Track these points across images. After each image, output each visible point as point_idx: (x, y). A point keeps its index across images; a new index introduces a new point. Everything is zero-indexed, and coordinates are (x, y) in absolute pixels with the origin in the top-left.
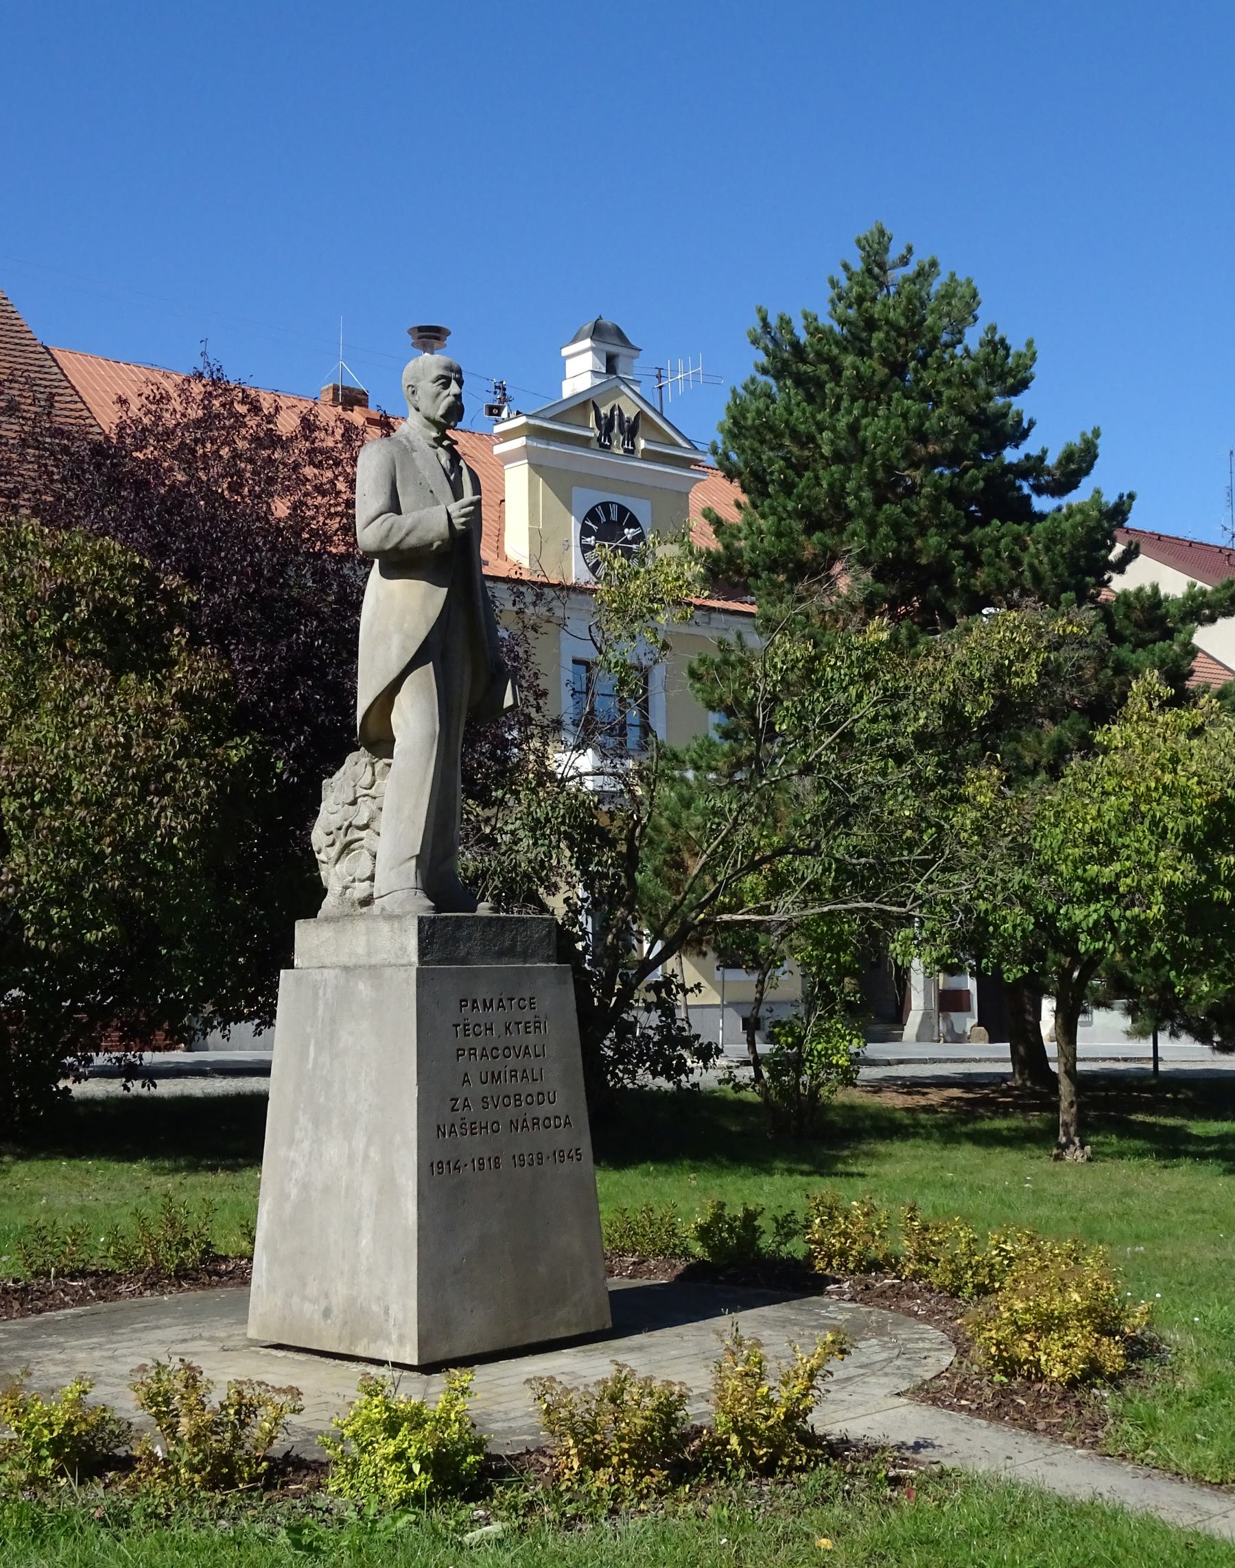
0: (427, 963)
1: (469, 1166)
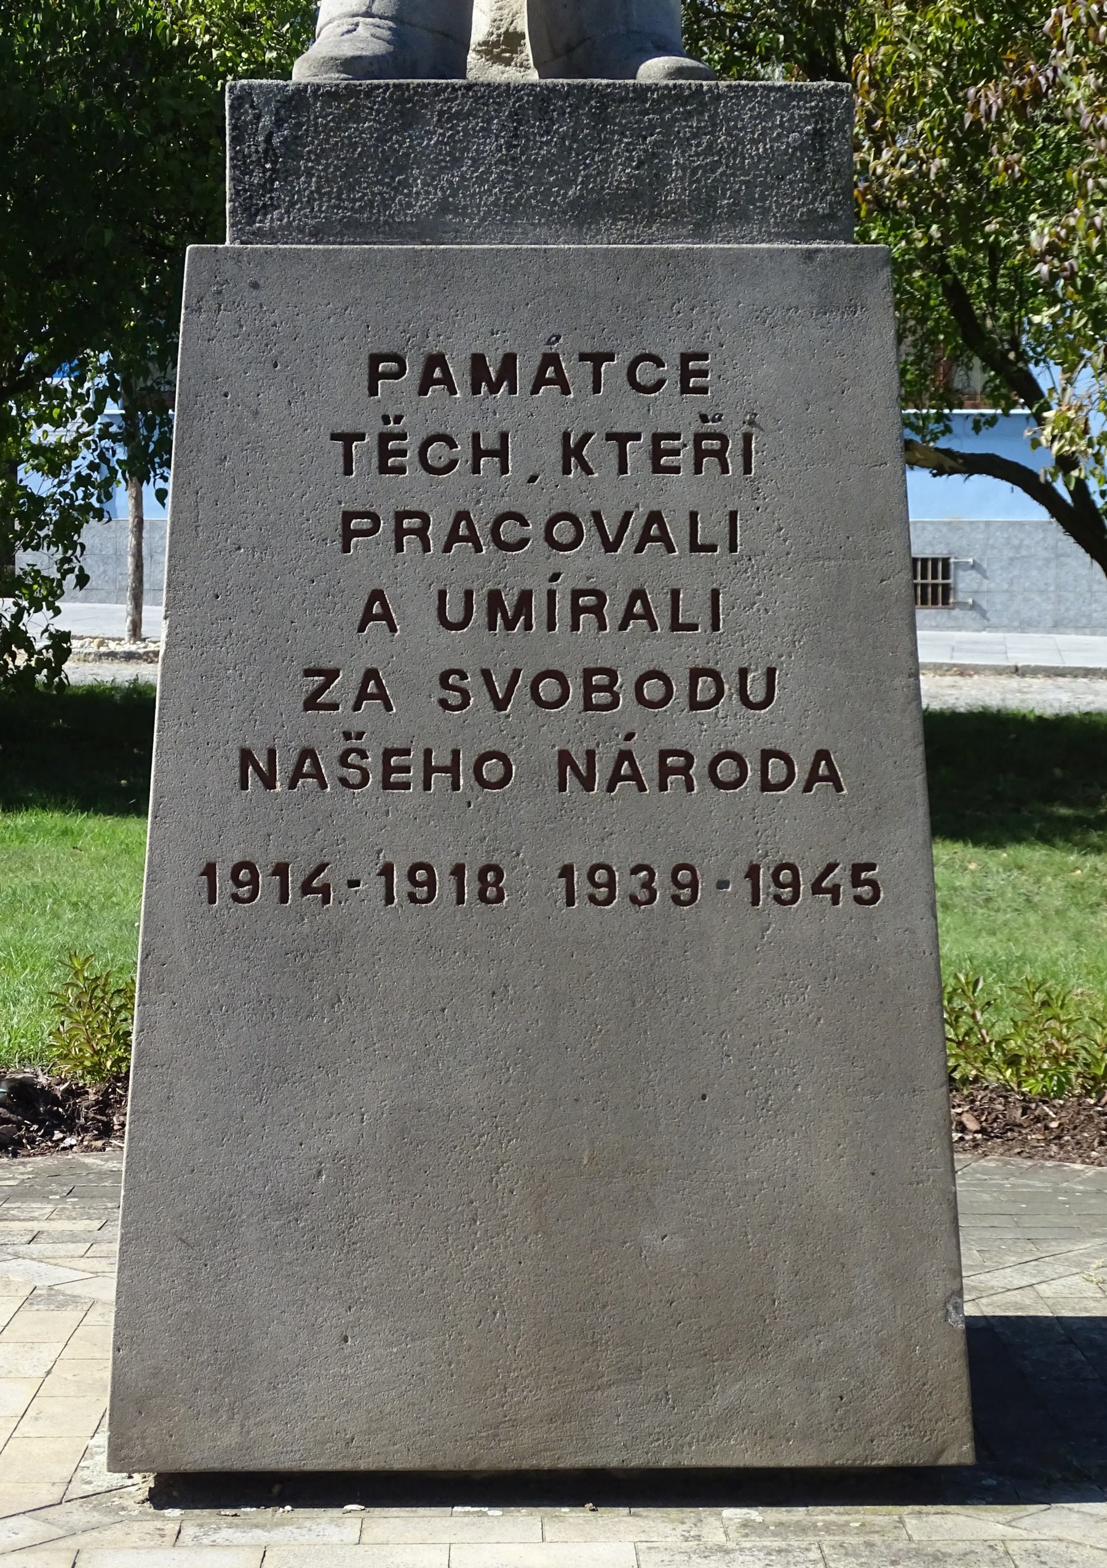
0: (260, 235)
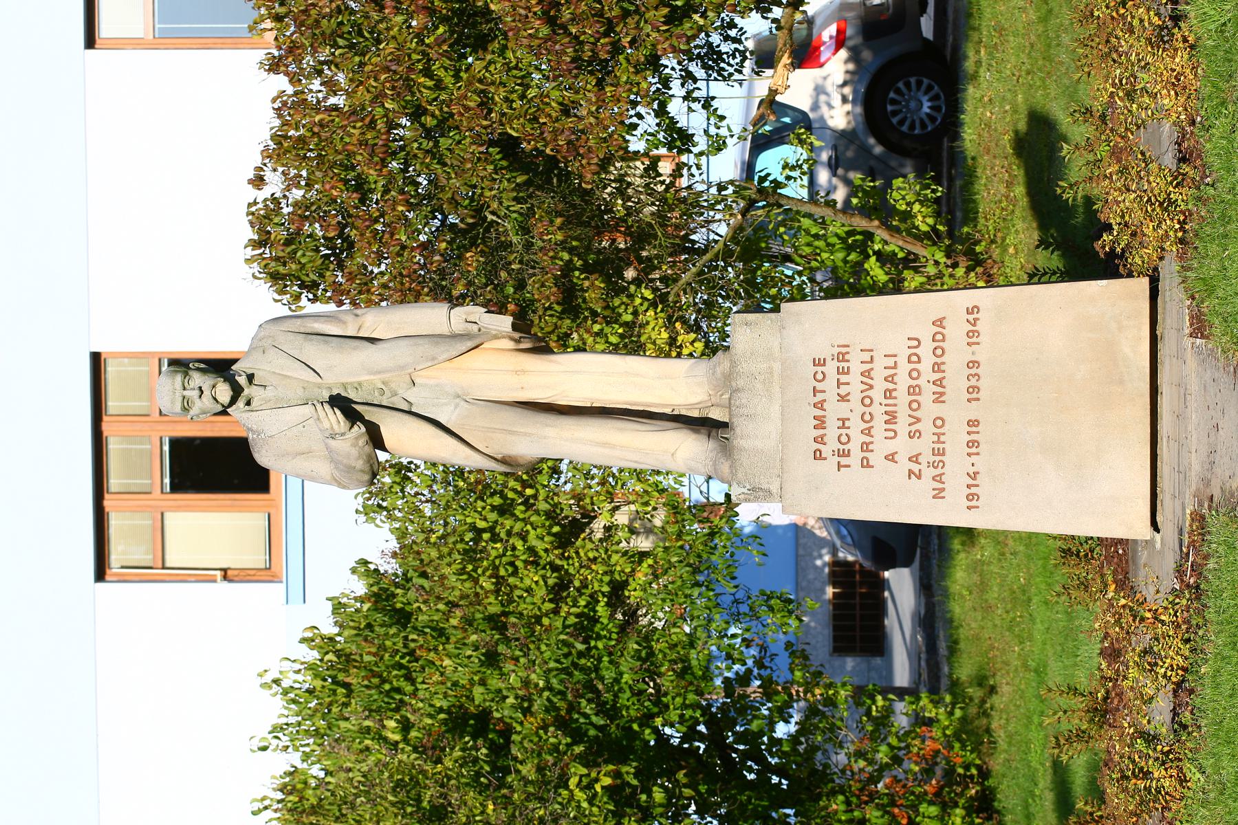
1: (974, 459)
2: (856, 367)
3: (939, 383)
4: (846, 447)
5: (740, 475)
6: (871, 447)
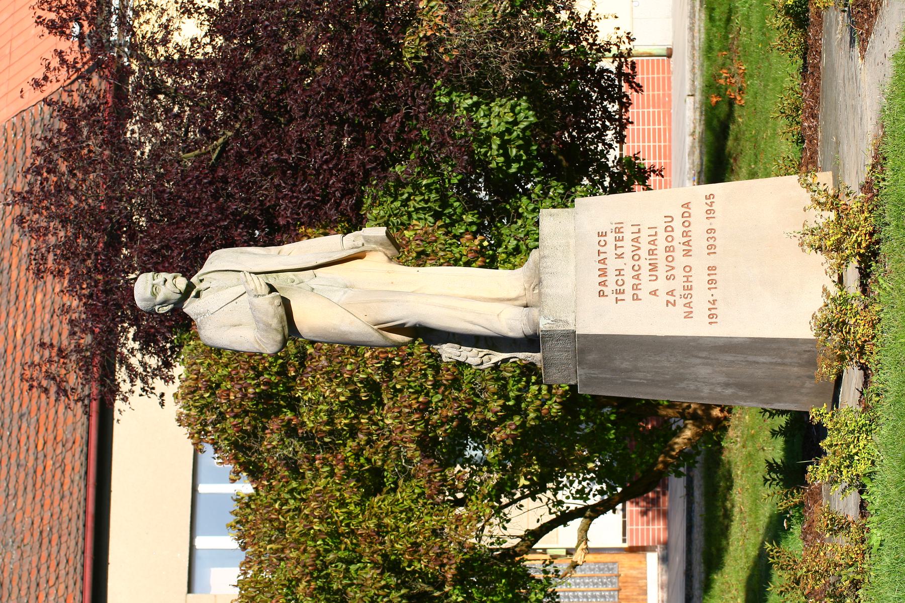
2: (628, 236)
3: (687, 243)
4: (622, 288)
5: (546, 312)
6: (639, 287)
